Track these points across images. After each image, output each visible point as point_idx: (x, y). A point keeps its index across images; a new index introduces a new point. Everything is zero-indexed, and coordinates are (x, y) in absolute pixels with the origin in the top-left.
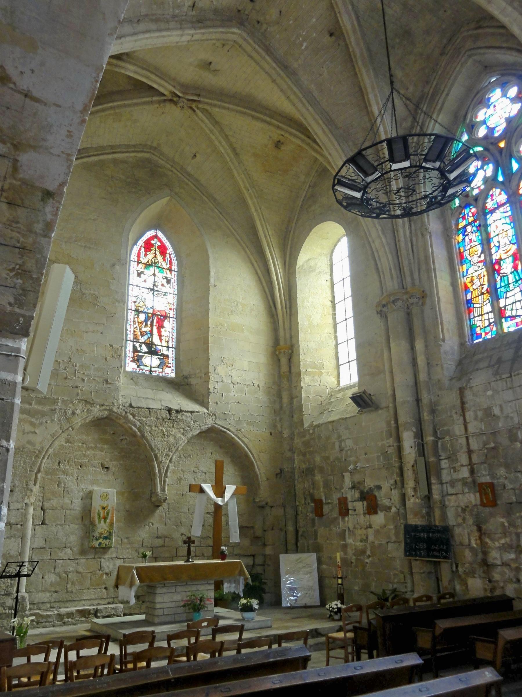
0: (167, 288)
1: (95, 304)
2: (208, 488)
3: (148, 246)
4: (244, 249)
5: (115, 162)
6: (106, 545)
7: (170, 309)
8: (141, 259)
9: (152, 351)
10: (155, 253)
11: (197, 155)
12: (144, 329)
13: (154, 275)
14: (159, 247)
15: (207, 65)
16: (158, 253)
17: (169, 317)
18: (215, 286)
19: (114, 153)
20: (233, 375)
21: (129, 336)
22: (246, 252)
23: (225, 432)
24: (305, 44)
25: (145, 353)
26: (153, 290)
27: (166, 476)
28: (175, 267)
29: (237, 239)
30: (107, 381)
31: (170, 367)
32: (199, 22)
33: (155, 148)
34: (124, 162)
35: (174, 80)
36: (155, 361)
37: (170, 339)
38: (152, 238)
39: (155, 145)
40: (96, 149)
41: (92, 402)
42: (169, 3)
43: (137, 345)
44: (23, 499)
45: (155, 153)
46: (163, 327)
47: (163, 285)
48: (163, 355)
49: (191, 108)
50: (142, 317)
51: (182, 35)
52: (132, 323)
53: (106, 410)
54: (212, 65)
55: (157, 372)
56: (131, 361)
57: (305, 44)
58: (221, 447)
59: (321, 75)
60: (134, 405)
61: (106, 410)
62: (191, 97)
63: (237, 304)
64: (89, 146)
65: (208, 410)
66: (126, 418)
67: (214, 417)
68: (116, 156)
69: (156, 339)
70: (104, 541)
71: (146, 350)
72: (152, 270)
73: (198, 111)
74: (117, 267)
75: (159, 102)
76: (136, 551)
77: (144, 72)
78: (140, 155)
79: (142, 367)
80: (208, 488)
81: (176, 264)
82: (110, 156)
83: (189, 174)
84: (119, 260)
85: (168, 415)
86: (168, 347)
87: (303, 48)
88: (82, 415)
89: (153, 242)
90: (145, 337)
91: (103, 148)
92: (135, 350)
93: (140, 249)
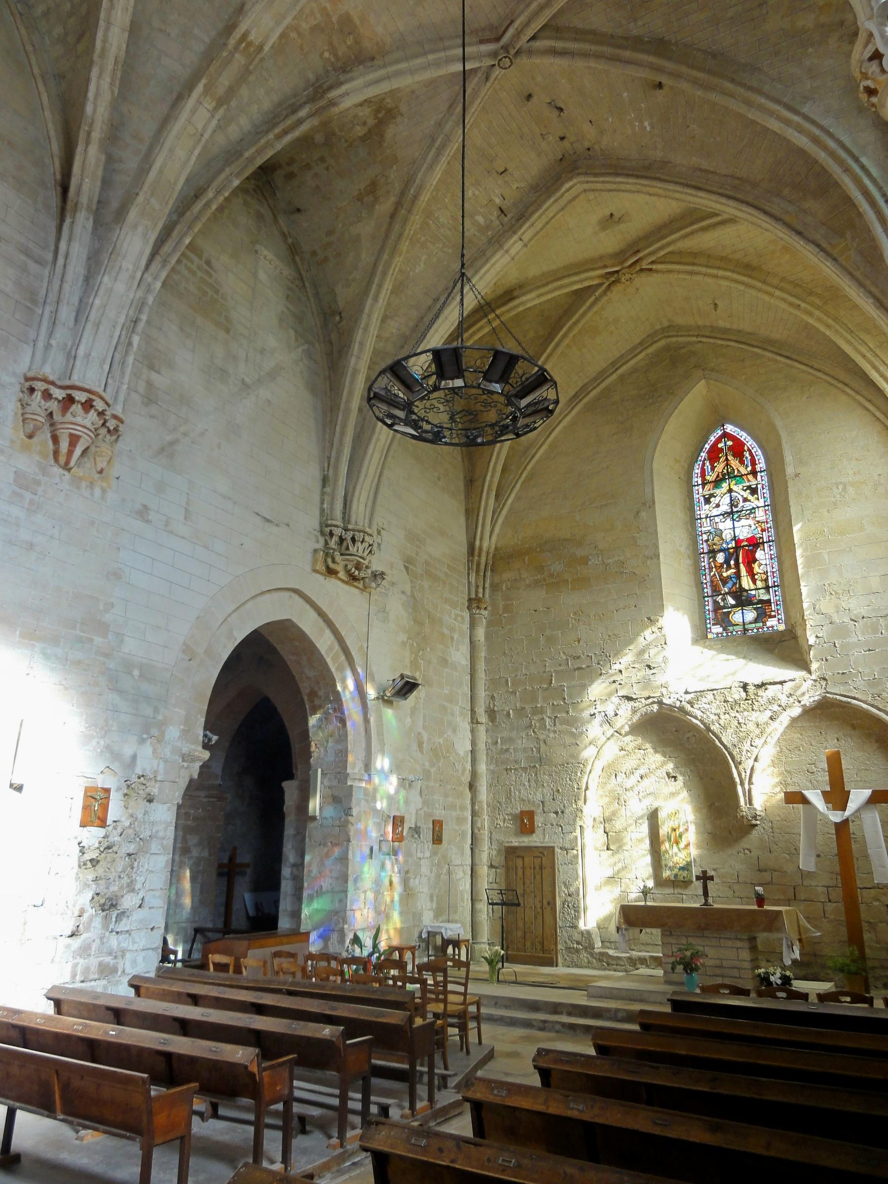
0: (754, 502)
1: (622, 573)
2: (815, 798)
3: (714, 455)
4: (844, 392)
5: (622, 378)
6: (684, 877)
7: (763, 530)
8: (708, 478)
9: (743, 599)
10: (727, 459)
11: (717, 302)
12: (725, 575)
13: (730, 491)
14: (730, 448)
15: (610, 221)
16: (730, 458)
17: (763, 543)
18: (797, 475)
19: (617, 369)
20: (852, 606)
21: (705, 590)
22: (847, 394)
23: (849, 703)
24: (646, 124)
25: (733, 606)
26: (732, 513)
27: (750, 783)
28: (761, 465)
29: (827, 382)
30: (649, 667)
31: (775, 616)
32: (518, 220)
33: (669, 327)
34: (634, 370)
35: (601, 258)
36: (750, 615)
37: (769, 574)
38: (718, 440)
39: (666, 324)
40: (595, 379)
41: (634, 697)
42: (475, 235)
43: (719, 599)
44: (575, 821)
45: (670, 334)
46: (755, 560)
47: (746, 500)
48: (761, 601)
49: (642, 270)
50: (720, 557)
51: (507, 251)
52: (707, 571)
53: (653, 703)
54: (615, 213)
55: (754, 630)
56: (714, 625)
57: (646, 124)
58: (854, 727)
59: (694, 137)
60: (689, 690)
61: (653, 703)
62: (629, 261)
63: (844, 488)
64: (586, 381)
65: (810, 672)
66: (682, 709)
67: (824, 683)
68: (620, 372)
69: (746, 583)
70: (681, 872)
71: (731, 601)
72: (725, 486)
73: (654, 267)
74: (643, 514)
75: (605, 293)
76: (730, 887)
77: (550, 287)
78: (650, 350)
79: (731, 628)
80: (815, 798)
81: (762, 460)
82: (614, 376)
83: (725, 331)
84: (644, 504)
85: (744, 695)
86: (767, 588)
87: (648, 129)
88: (625, 715)
89: (720, 446)
90: (730, 585)
91: (603, 372)
92: (717, 607)
93: (704, 464)
